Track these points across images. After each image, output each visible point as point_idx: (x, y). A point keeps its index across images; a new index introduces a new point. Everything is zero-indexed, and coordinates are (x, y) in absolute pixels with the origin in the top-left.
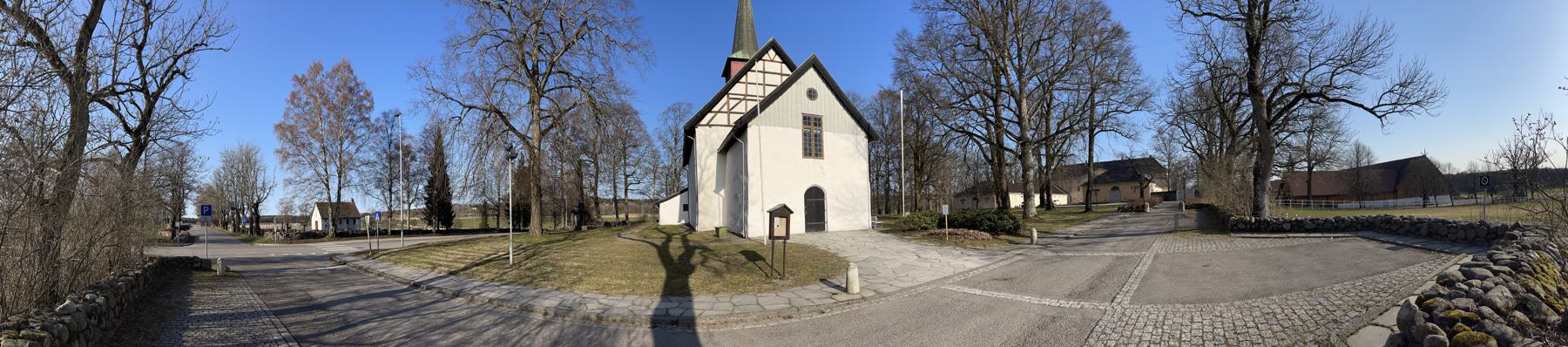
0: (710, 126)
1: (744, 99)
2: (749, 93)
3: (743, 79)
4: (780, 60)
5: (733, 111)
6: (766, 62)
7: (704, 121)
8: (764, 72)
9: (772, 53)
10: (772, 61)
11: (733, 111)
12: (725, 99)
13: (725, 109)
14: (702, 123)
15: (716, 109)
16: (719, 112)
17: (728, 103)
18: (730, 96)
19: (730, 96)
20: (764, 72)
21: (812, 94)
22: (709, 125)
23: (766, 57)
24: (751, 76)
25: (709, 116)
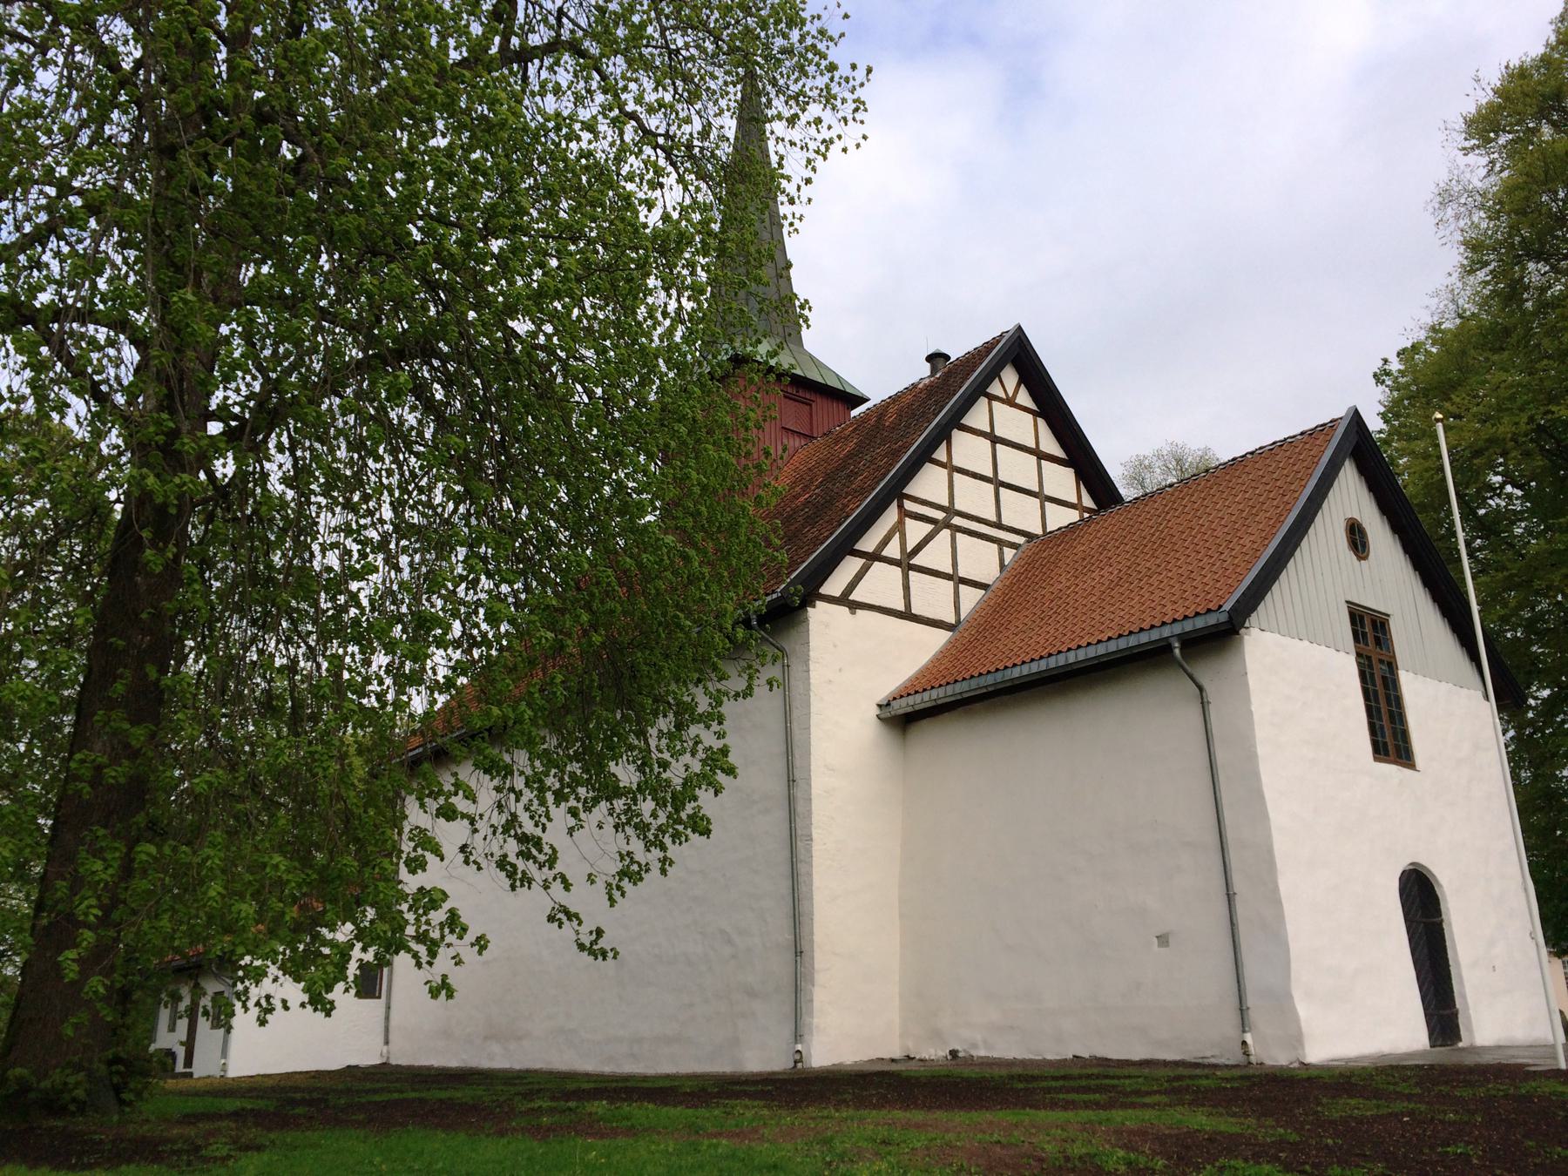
0: (855, 606)
1: (947, 525)
2: (958, 506)
3: (941, 454)
4: (1030, 404)
5: (916, 561)
6: (995, 404)
7: (834, 585)
8: (995, 440)
9: (1010, 377)
10: (1010, 402)
11: (916, 561)
12: (891, 516)
13: (893, 550)
14: (824, 590)
15: (868, 543)
16: (875, 557)
17: (899, 528)
18: (909, 505)
19: (909, 505)
20: (995, 440)
21: (1357, 538)
22: (844, 600)
23: (995, 389)
24: (968, 450)
25: (851, 566)
